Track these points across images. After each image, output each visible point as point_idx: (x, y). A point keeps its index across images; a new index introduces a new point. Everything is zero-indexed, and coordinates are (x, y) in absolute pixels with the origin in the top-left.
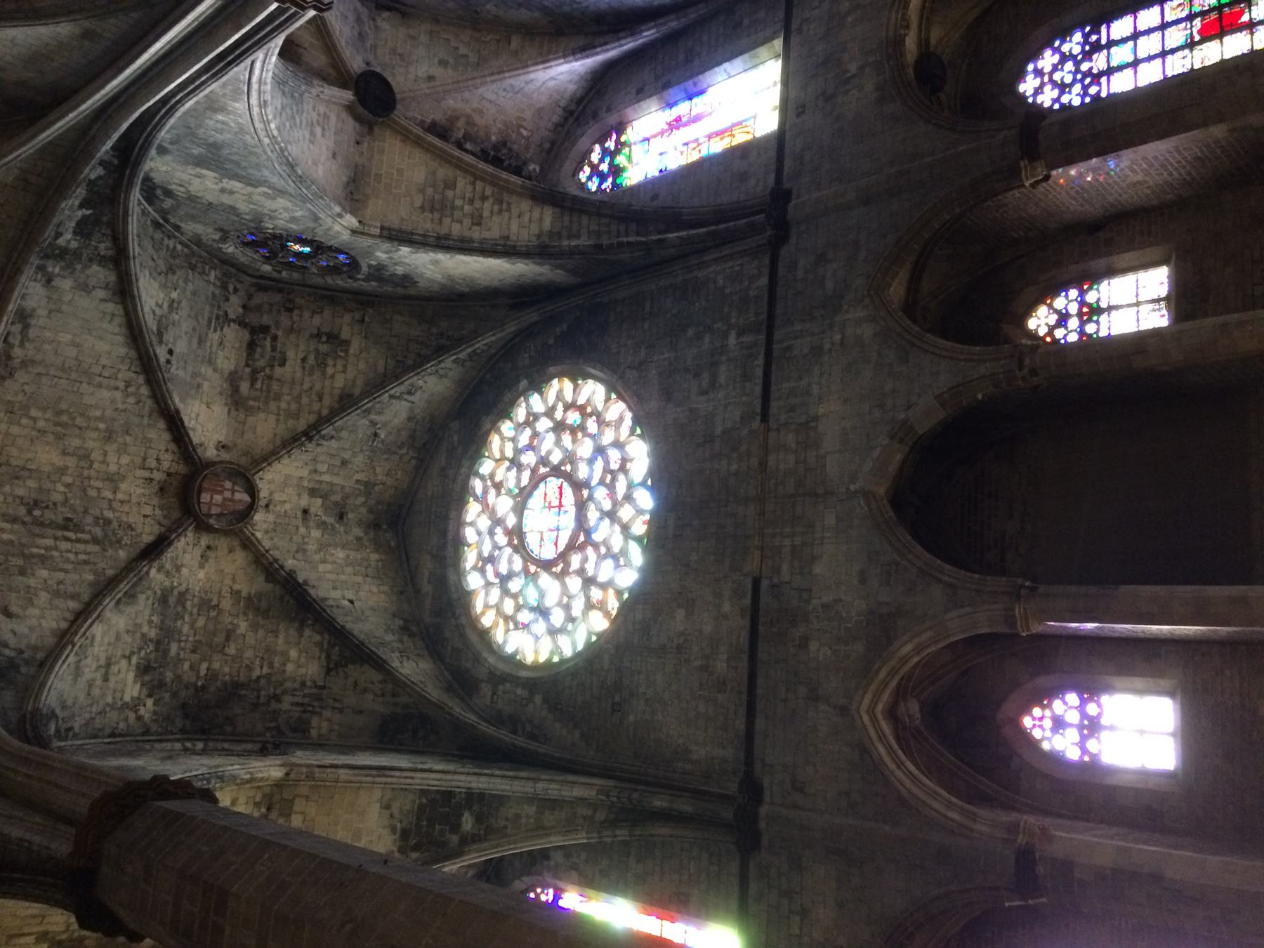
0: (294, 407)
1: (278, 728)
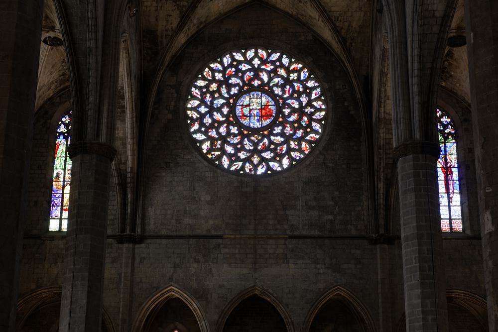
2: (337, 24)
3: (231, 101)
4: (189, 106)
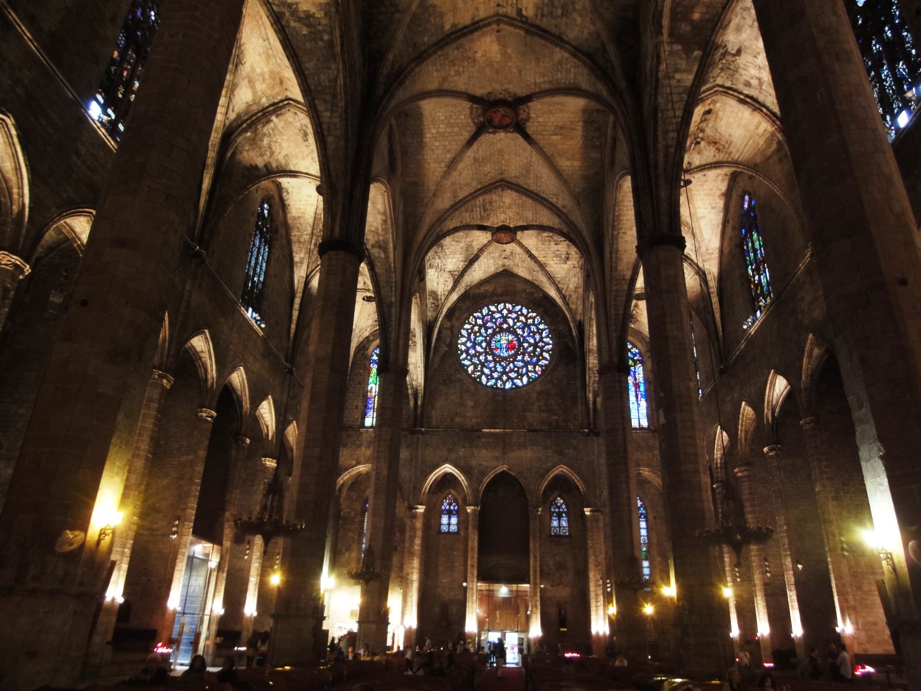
0: (540, 249)
1: (430, 260)
2: (560, 286)
3: (488, 338)
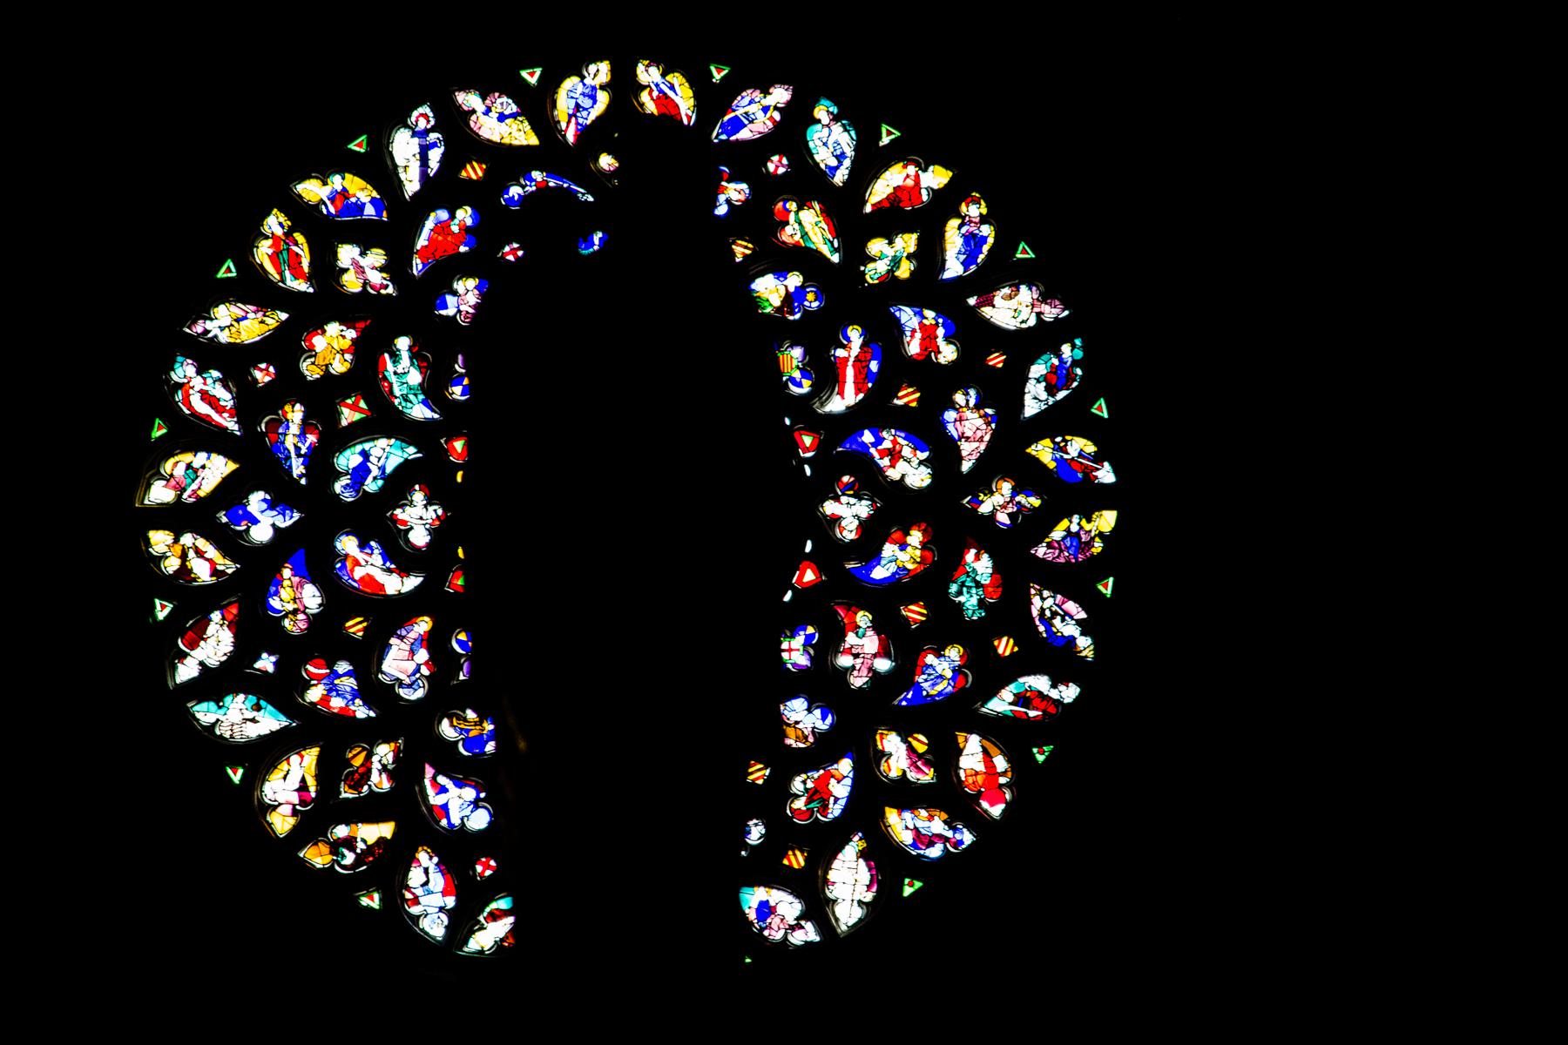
4: (159, 494)
